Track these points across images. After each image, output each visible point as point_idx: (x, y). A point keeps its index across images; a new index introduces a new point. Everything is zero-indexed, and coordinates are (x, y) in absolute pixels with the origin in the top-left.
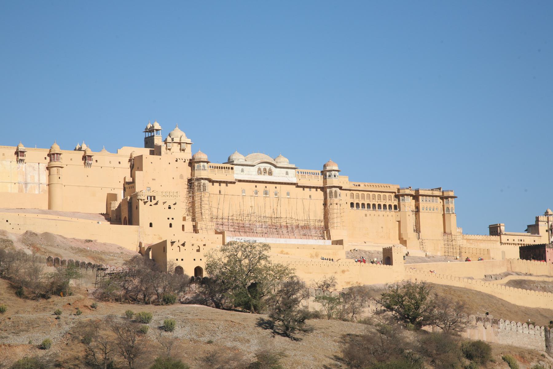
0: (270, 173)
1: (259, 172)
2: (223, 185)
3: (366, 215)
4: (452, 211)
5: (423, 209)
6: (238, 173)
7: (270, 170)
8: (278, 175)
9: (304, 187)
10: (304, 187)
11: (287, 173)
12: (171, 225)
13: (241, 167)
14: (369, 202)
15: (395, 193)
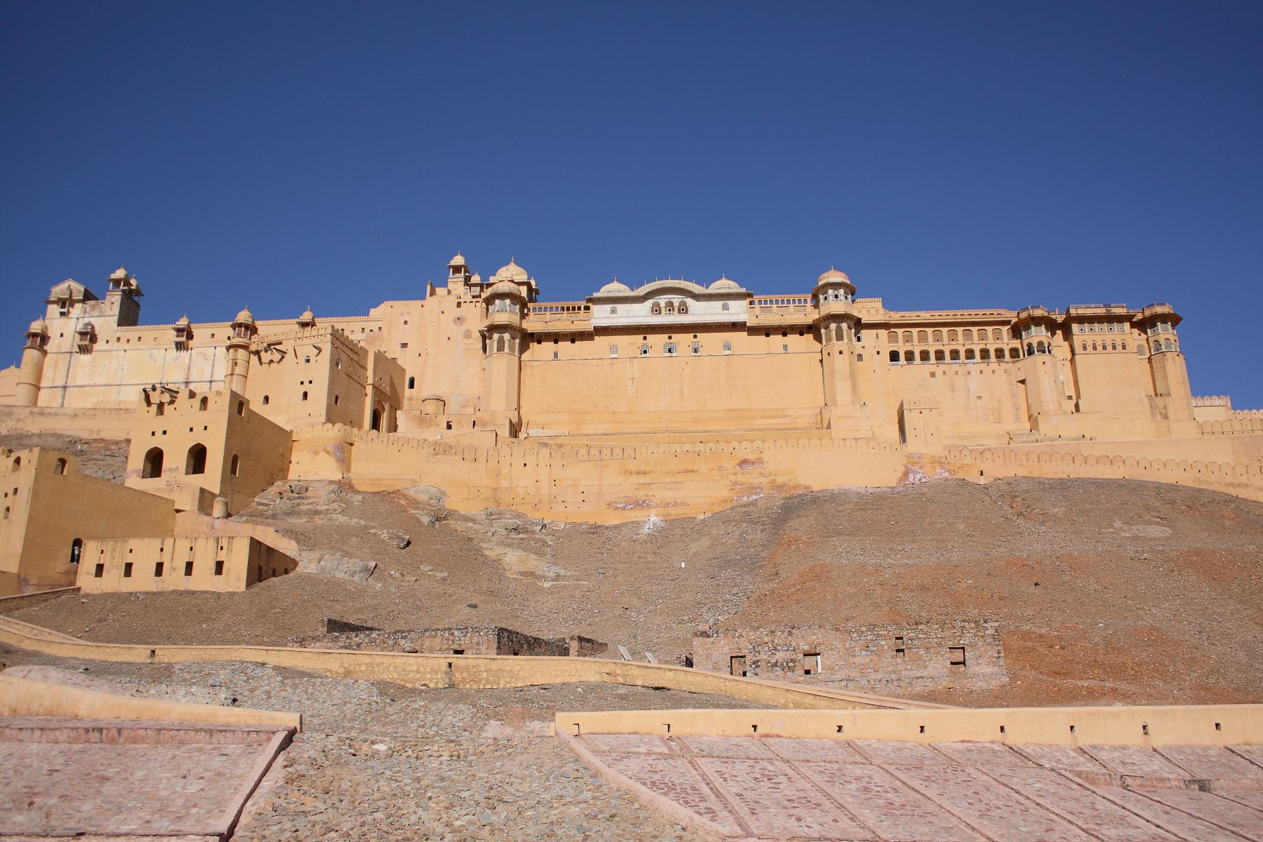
0: (683, 309)
1: (656, 310)
2: (564, 346)
3: (933, 375)
4: (1168, 346)
5: (1085, 348)
6: (601, 315)
7: (683, 304)
8: (701, 312)
9: (767, 331)
10: (767, 331)
11: (725, 307)
12: (305, 395)
13: (609, 307)
14: (941, 348)
15: (1007, 323)
